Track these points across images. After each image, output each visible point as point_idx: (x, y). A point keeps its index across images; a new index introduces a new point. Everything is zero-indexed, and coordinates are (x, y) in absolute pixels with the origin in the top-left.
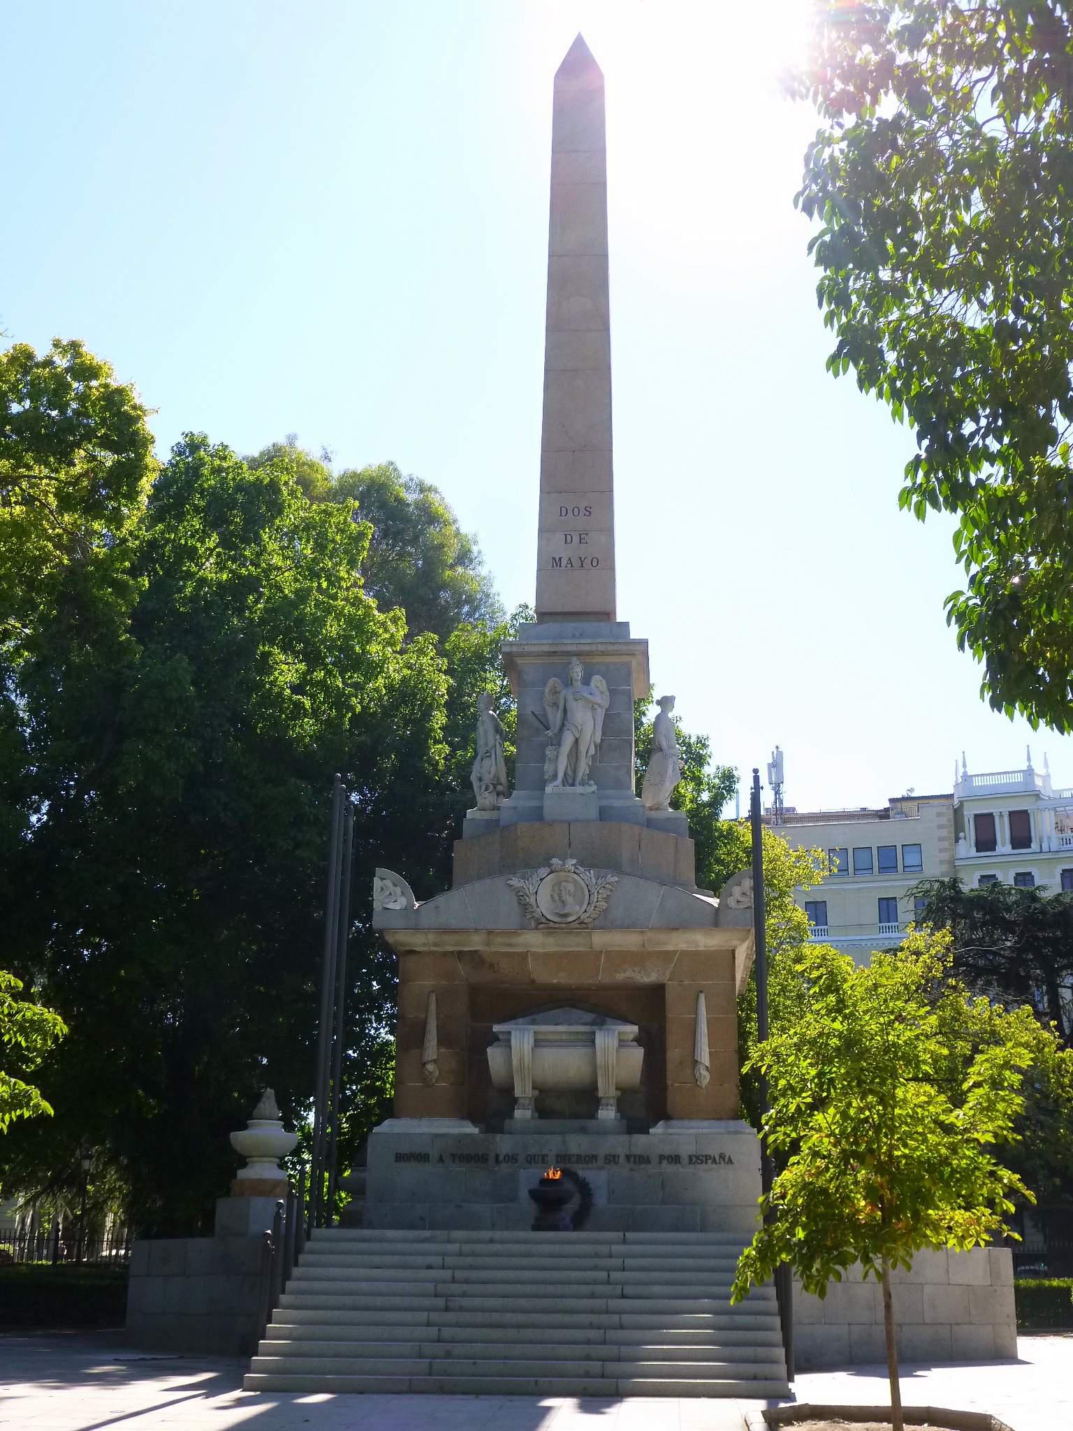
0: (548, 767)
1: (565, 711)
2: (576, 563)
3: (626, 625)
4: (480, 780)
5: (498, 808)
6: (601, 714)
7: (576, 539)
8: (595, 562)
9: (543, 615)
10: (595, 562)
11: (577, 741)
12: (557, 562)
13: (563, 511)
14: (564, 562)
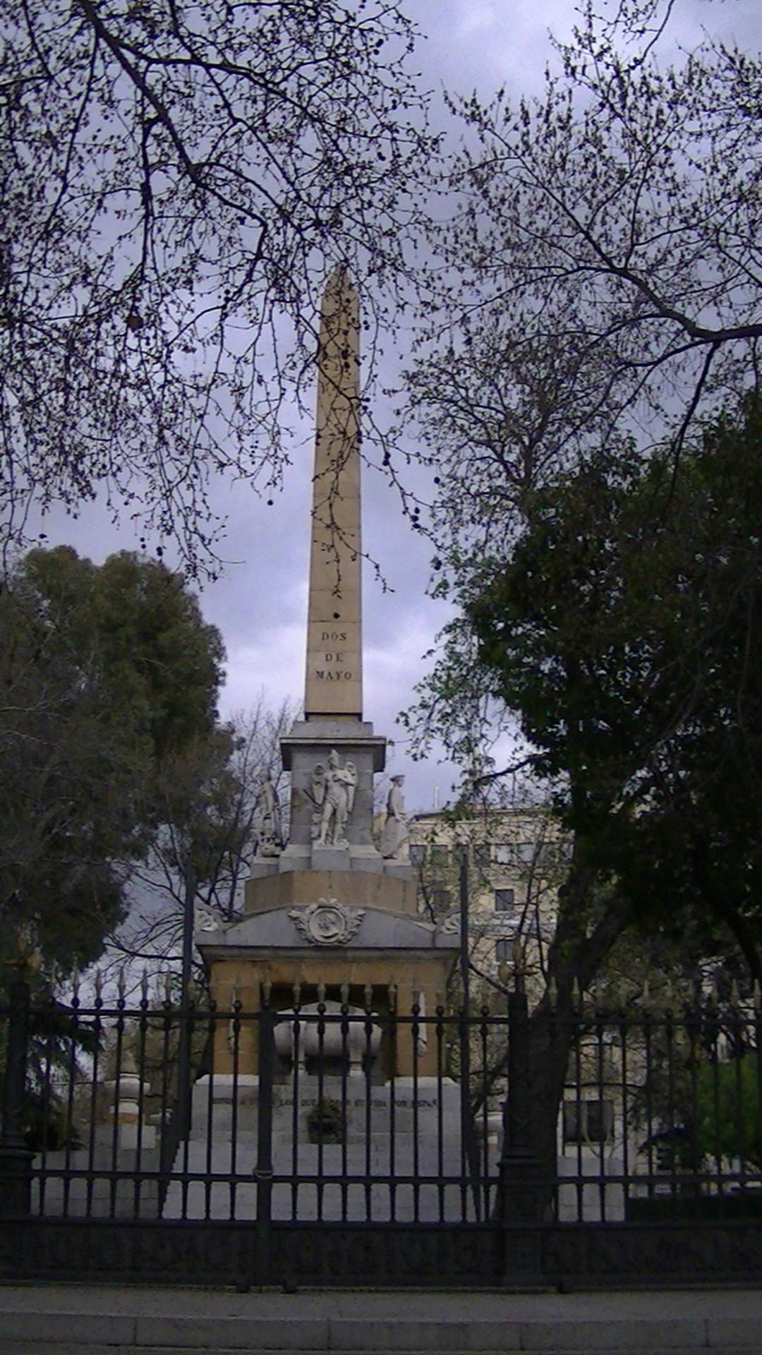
0: (315, 830)
1: (327, 788)
2: (335, 677)
3: (370, 724)
4: (263, 834)
5: (277, 856)
6: (351, 789)
7: (334, 658)
8: (348, 676)
9: (308, 715)
10: (348, 676)
11: (334, 813)
12: (320, 674)
13: (325, 636)
14: (325, 675)
